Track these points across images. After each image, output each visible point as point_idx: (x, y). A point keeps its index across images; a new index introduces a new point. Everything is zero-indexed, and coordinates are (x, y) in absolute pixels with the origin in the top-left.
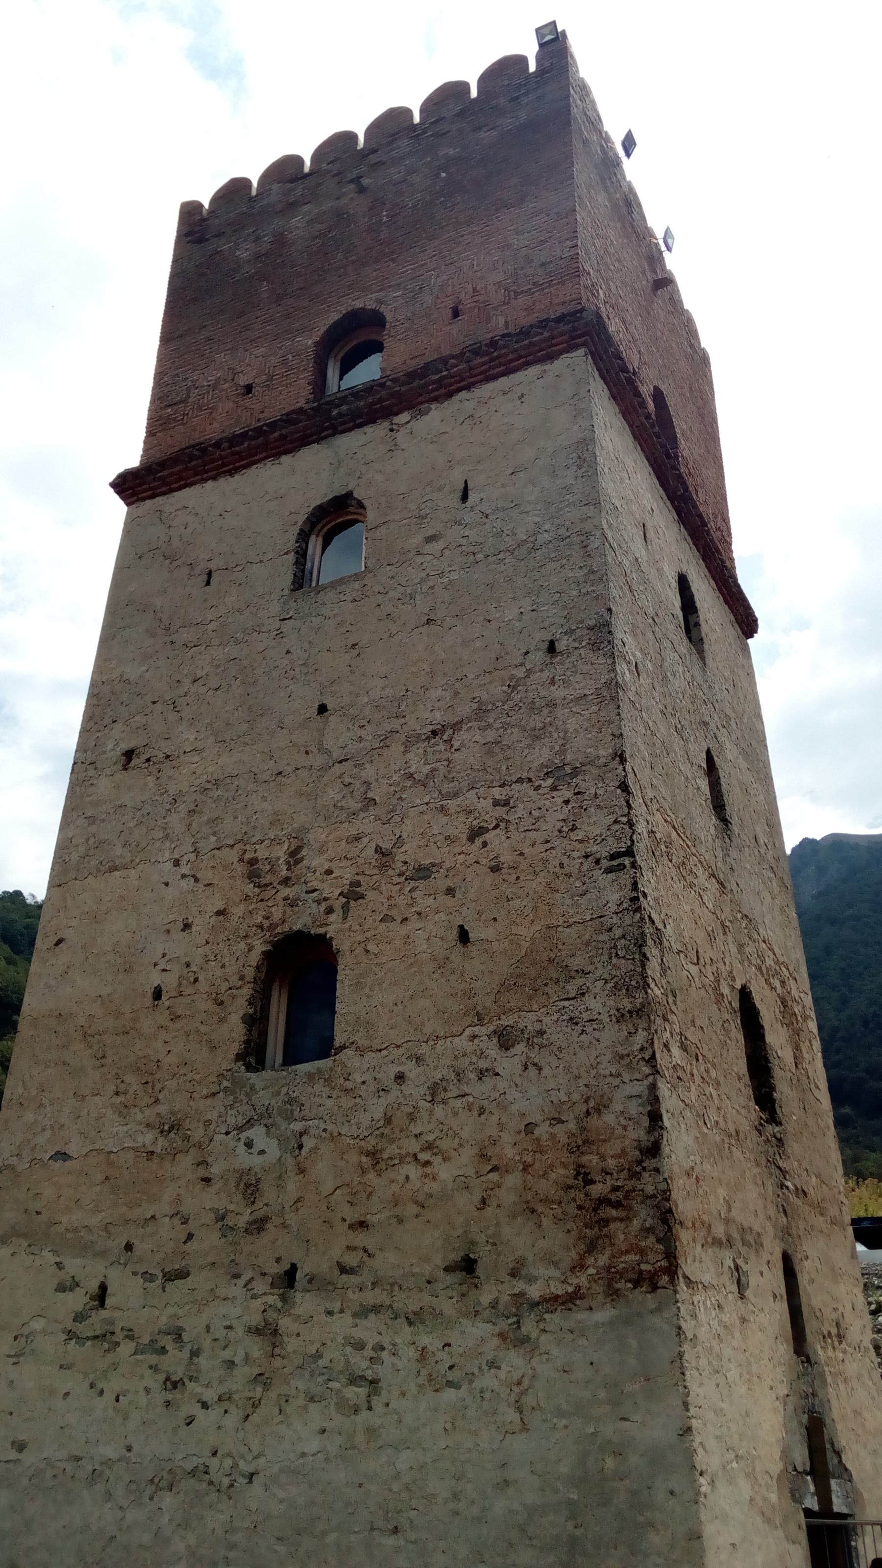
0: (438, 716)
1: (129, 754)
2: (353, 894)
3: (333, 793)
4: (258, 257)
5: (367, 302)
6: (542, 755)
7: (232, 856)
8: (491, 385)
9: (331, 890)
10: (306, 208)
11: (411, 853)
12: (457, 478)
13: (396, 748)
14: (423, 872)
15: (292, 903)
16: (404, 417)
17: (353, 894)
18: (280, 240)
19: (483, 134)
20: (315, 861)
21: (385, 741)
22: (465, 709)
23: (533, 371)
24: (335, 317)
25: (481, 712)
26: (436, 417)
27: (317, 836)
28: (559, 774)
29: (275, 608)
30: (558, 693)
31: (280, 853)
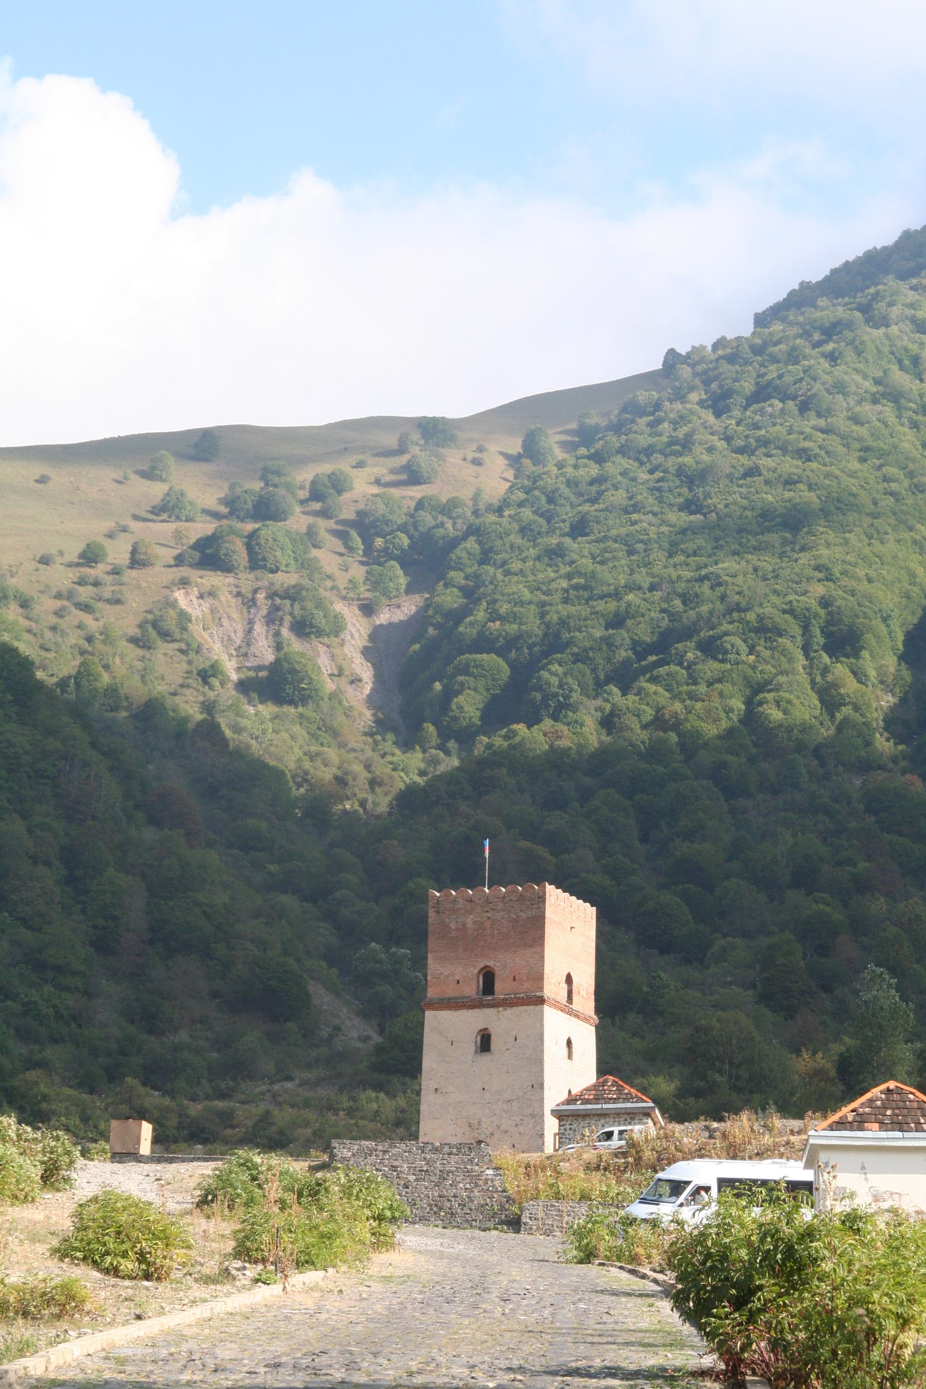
0: (509, 1097)
1: (436, 1090)
2: (492, 1134)
3: (487, 1110)
4: (457, 930)
5: (491, 963)
6: (529, 1111)
7: (465, 1120)
8: (522, 1008)
9: (488, 1133)
10: (472, 917)
11: (504, 1127)
12: (514, 1033)
13: (500, 1103)
14: (506, 1132)
15: (479, 1134)
16: (501, 1009)
17: (492, 1134)
18: (464, 924)
19: (522, 914)
20: (484, 1125)
21: (498, 1100)
22: (515, 1097)
23: (532, 1007)
24: (482, 965)
25: (518, 1098)
26: (510, 1012)
27: (484, 1120)
28: (533, 1116)
29: (470, 1057)
30: (533, 1098)
31: (476, 1122)
